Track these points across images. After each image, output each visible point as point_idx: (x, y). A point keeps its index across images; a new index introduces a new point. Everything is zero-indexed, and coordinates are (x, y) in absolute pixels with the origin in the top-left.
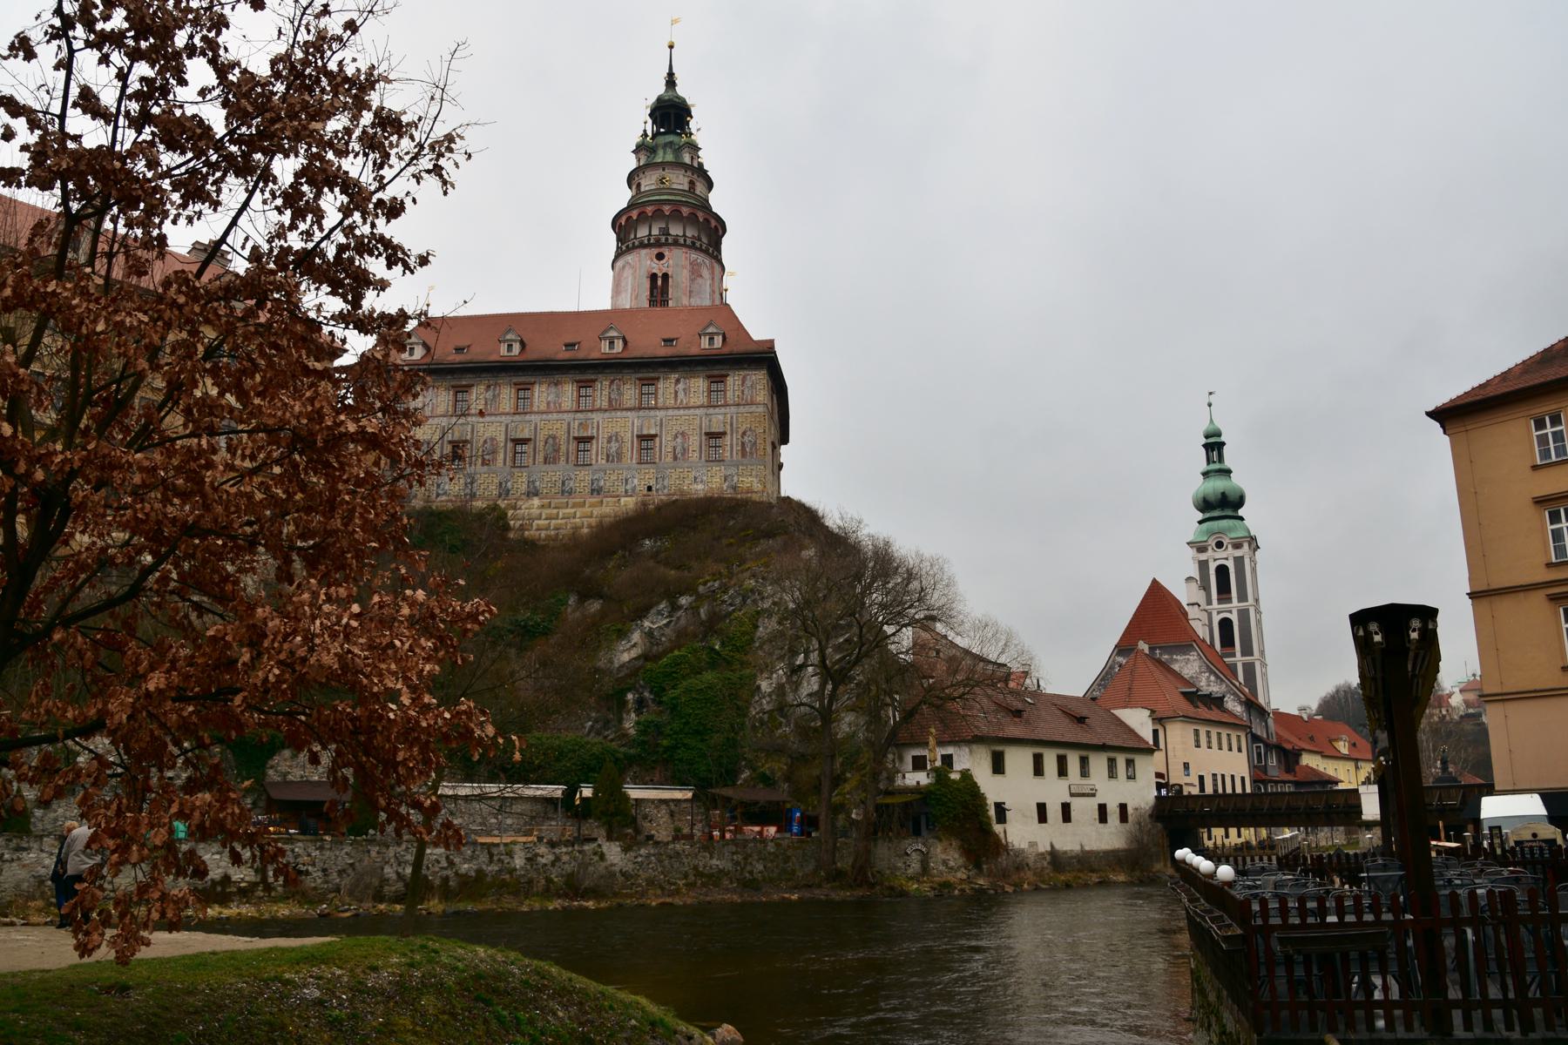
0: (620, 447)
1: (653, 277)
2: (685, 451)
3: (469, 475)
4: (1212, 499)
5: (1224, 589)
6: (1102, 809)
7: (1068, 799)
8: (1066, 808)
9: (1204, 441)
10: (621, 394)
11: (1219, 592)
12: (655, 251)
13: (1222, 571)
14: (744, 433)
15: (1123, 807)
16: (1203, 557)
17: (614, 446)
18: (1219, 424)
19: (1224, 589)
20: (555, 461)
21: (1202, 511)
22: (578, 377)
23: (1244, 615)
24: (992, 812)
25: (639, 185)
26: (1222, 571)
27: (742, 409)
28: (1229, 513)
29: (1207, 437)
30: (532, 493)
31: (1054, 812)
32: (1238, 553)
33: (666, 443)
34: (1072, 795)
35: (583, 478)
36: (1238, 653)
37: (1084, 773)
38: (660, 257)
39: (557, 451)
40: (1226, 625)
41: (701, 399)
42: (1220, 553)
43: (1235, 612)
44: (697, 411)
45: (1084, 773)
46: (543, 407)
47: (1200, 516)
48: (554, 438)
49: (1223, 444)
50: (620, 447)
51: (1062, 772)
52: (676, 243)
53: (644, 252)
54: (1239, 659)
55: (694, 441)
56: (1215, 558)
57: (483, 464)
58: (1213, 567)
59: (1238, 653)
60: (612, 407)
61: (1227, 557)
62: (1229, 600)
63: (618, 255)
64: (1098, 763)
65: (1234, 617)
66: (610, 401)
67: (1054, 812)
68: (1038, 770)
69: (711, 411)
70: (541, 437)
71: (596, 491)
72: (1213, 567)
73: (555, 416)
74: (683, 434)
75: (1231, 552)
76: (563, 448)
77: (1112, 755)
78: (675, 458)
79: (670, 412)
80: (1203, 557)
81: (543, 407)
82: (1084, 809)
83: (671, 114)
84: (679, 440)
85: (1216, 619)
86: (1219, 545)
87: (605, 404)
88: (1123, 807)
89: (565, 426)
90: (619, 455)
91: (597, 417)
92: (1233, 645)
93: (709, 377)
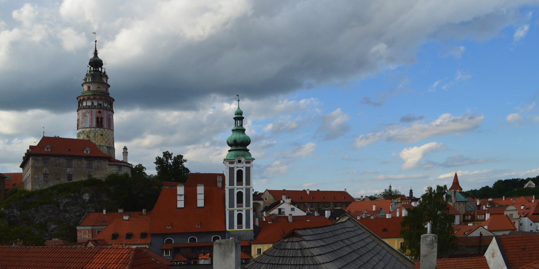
4: (238, 142)
5: (240, 180)
11: (237, 181)
13: (240, 172)
19: (240, 180)
26: (240, 172)
28: (242, 148)
36: (244, 206)
42: (240, 165)
43: (244, 189)
47: (230, 148)
59: (244, 206)
61: (243, 167)
62: (242, 185)
65: (244, 192)
75: (245, 165)
80: (232, 166)
85: (236, 192)
86: (240, 161)
92: (242, 202)
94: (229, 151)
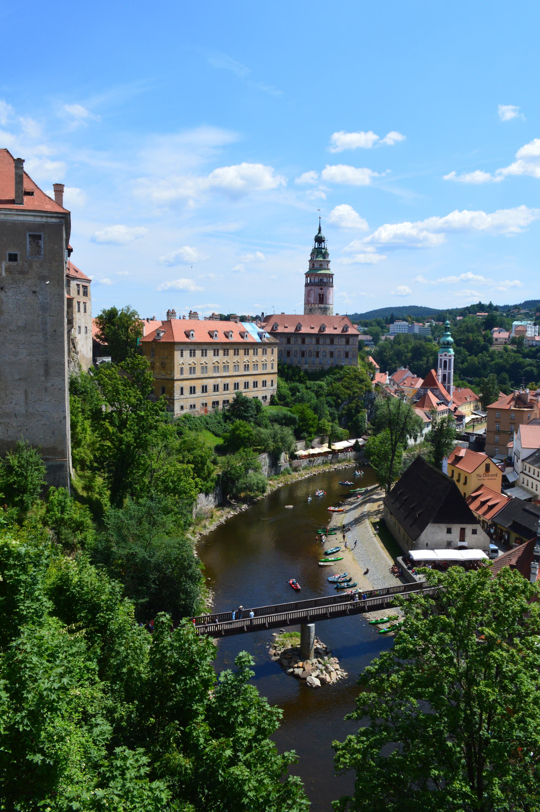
1: (320, 295)
13: (445, 362)
26: (445, 362)
30: (306, 363)
33: (336, 354)
35: (317, 361)
38: (321, 289)
41: (344, 343)
42: (445, 357)
55: (342, 353)
58: (443, 360)
60: (324, 344)
71: (321, 364)
72: (443, 360)
83: (319, 240)
91: (320, 346)
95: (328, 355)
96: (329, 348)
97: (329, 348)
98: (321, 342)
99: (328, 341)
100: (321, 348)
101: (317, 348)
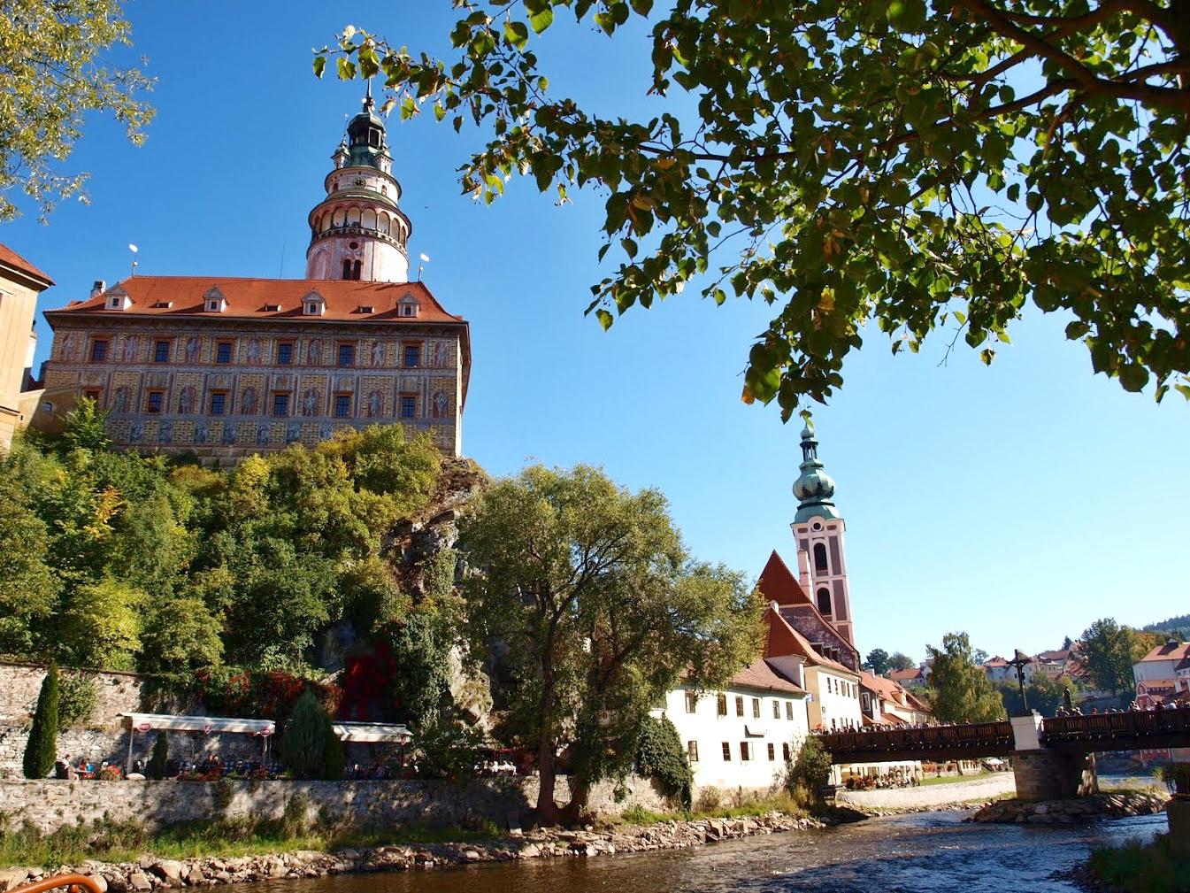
0: (317, 402)
1: (347, 263)
2: (379, 408)
3: (164, 422)
6: (771, 746)
7: (745, 740)
8: (744, 746)
9: (801, 441)
10: (320, 353)
12: (349, 240)
13: (819, 549)
14: (436, 395)
15: (786, 746)
16: (804, 536)
17: (311, 402)
18: (811, 430)
20: (252, 411)
21: (800, 499)
22: (278, 336)
23: (839, 586)
24: (686, 749)
25: (336, 186)
26: (819, 549)
27: (434, 373)
29: (803, 438)
31: (735, 751)
32: (833, 533)
33: (360, 402)
34: (748, 734)
37: (757, 715)
38: (354, 246)
39: (255, 402)
40: (823, 594)
41: (398, 361)
42: (818, 534)
44: (392, 373)
45: (757, 715)
46: (243, 360)
48: (253, 390)
49: (816, 443)
50: (317, 402)
51: (740, 713)
52: (367, 235)
53: (339, 241)
54: (835, 623)
55: (389, 401)
56: (813, 538)
57: (180, 411)
60: (312, 364)
61: (823, 537)
63: (312, 245)
64: (766, 702)
66: (309, 358)
67: (735, 751)
68: (722, 709)
69: (406, 373)
70: (240, 388)
72: (812, 545)
73: (254, 370)
74: (378, 393)
76: (261, 400)
77: (776, 699)
78: (370, 414)
79: (367, 372)
80: (804, 536)
81: (243, 360)
82: (758, 748)
84: (374, 398)
86: (817, 526)
87: (304, 361)
88: (786, 746)
89: (264, 380)
90: (316, 410)
91: (295, 373)
93: (404, 342)
94: (799, 508)
95: (327, 408)
96: (330, 381)
97: (330, 381)
98: (300, 354)
99: (329, 353)
100: (299, 380)
101: (281, 380)
